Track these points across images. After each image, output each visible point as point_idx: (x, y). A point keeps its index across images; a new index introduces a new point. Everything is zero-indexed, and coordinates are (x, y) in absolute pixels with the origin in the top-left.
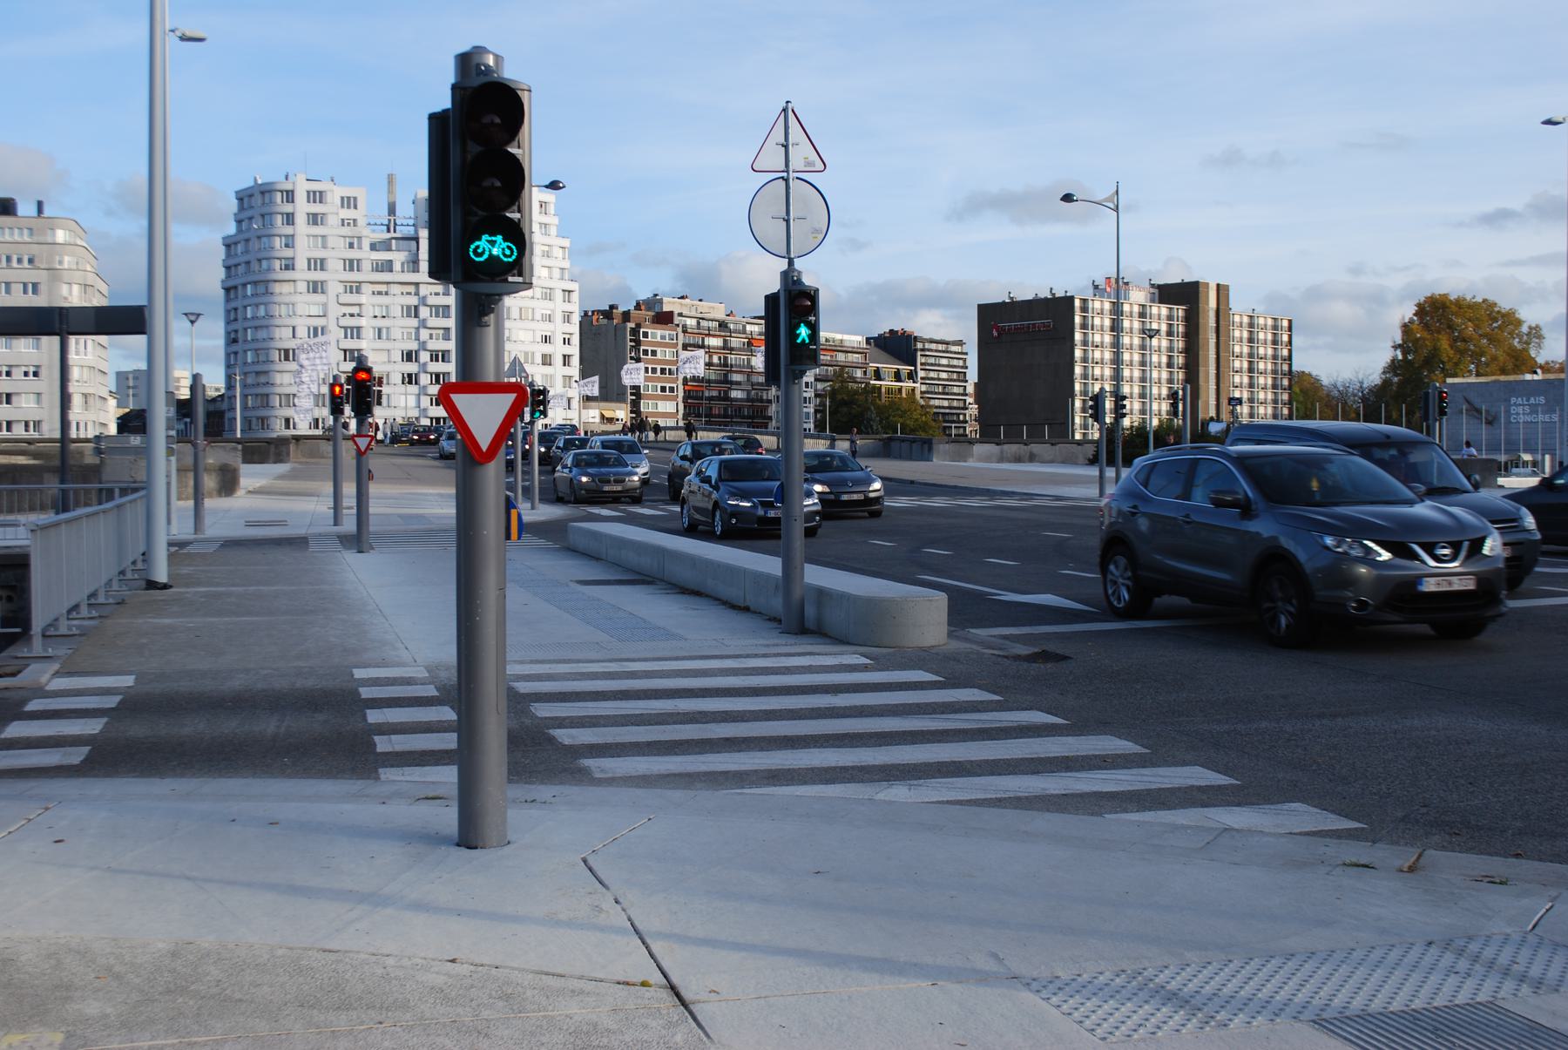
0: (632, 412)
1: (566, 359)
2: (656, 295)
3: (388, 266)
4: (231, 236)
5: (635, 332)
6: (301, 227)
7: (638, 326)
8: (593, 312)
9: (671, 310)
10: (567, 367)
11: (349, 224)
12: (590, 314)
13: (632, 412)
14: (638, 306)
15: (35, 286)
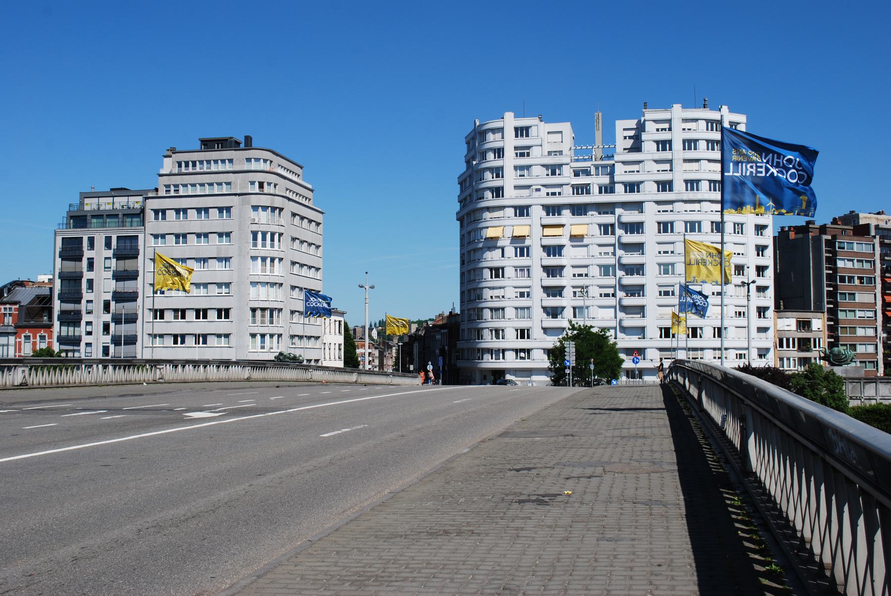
0: (829, 320)
1: (760, 270)
2: (853, 212)
3: (583, 189)
4: (465, 172)
5: (831, 244)
6: (510, 160)
7: (834, 237)
8: (790, 227)
9: (868, 223)
10: (761, 277)
11: (556, 155)
12: (787, 229)
13: (829, 320)
14: (835, 222)
15: (228, 209)
